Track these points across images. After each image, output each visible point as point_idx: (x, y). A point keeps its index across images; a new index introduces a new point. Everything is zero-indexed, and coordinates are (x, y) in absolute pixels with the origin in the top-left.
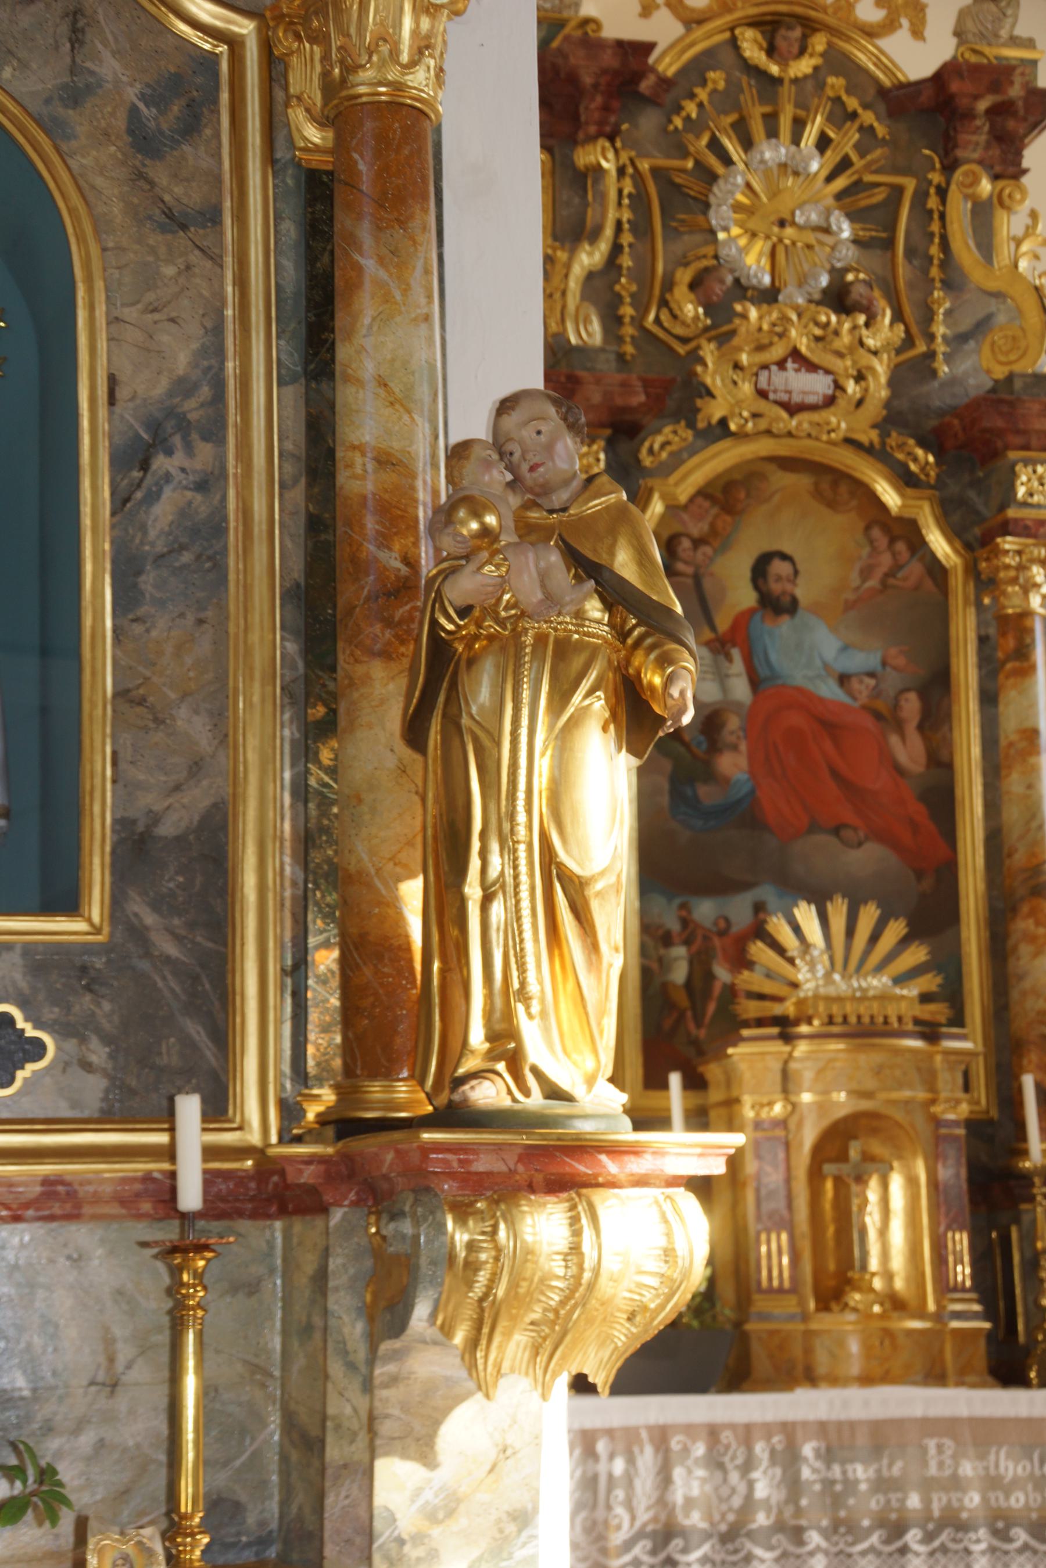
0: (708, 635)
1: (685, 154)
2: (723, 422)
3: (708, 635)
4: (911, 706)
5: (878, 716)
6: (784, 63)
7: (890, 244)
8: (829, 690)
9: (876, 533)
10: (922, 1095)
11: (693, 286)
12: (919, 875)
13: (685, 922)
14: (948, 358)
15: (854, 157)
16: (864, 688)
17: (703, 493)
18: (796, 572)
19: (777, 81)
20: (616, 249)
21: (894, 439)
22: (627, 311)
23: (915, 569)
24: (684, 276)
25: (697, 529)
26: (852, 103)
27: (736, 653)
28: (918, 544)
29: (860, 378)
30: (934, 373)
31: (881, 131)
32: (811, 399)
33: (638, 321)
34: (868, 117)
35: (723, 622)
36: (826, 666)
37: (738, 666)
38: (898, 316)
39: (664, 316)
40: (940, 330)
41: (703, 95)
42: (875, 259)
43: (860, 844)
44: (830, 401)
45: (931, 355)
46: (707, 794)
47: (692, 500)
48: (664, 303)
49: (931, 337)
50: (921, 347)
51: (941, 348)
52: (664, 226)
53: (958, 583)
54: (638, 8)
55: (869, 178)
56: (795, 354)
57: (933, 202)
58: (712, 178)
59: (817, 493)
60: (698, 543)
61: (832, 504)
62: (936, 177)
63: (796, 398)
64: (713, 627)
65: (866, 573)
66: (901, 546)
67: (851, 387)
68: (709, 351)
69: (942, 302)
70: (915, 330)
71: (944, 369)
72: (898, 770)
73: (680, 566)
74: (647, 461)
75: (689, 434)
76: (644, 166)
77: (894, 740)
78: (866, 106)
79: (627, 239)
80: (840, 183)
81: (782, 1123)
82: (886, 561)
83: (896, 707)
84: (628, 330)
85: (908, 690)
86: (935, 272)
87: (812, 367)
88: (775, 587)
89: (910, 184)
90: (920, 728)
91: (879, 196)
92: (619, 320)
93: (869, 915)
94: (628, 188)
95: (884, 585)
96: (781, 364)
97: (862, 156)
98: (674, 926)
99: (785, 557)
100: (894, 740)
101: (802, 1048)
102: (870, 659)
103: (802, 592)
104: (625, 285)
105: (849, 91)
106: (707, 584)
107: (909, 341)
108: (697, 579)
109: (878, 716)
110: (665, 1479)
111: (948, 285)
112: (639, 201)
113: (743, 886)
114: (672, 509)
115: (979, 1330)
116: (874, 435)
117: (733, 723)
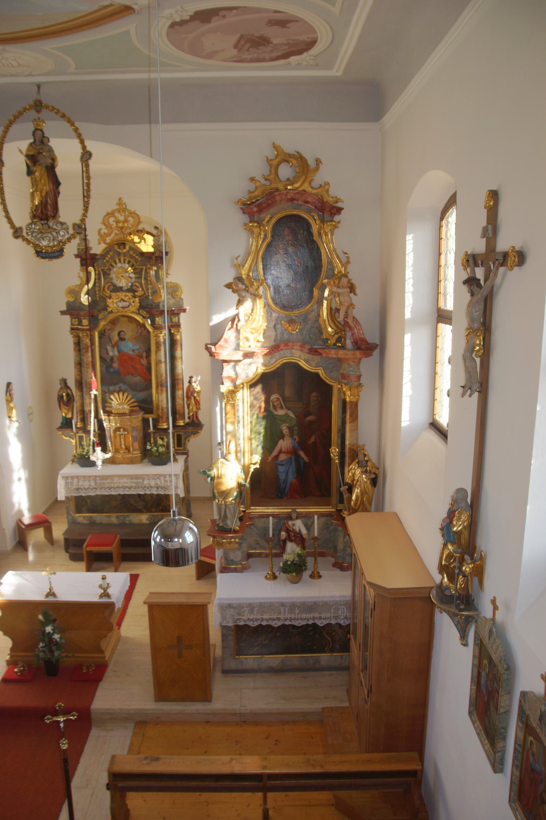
0: (111, 345)
1: (106, 267)
2: (112, 311)
3: (111, 345)
4: (144, 354)
5: (139, 356)
6: (122, 250)
7: (141, 278)
8: (131, 353)
9: (139, 326)
10: (130, 424)
11: (108, 288)
12: (146, 381)
13: (108, 390)
14: (151, 296)
15: (135, 264)
16: (136, 352)
17: (110, 322)
18: (125, 334)
19: (120, 253)
20: (95, 283)
21: (141, 311)
22: (97, 292)
23: (145, 332)
24: (107, 286)
25: (109, 328)
26: (134, 255)
27: (116, 347)
28: (145, 328)
29: (134, 302)
30: (149, 299)
31: (139, 259)
32: (126, 306)
33: (99, 294)
34: (137, 257)
35: (113, 342)
36: (130, 349)
37: (116, 350)
38: (143, 290)
39: (104, 293)
40: (150, 291)
41: (109, 256)
42: (138, 280)
43: (136, 377)
44: (129, 306)
45: (148, 296)
46: (111, 370)
47: (108, 323)
48: (104, 290)
49: (148, 293)
50: (147, 294)
51: (150, 294)
52: (104, 278)
53: (152, 335)
54: (98, 243)
55: (137, 267)
56: (122, 300)
57: (148, 271)
58: (110, 270)
59: (128, 321)
60: (109, 330)
61: (131, 322)
62: (149, 266)
63: (123, 306)
64: (111, 343)
65: (137, 333)
66: (143, 329)
67: (132, 303)
68: (108, 300)
69: (149, 286)
70: (146, 292)
71: (150, 298)
72: (142, 365)
73: (106, 334)
74: (100, 318)
75: (106, 313)
76: (100, 269)
77: (142, 360)
78: (137, 255)
79: (97, 281)
80: (133, 268)
81: (110, 428)
82: (140, 331)
83: (142, 355)
84: (98, 296)
85: (144, 352)
86: (149, 282)
87: (125, 301)
88: (122, 336)
89: (144, 268)
90: (146, 358)
91: (138, 270)
92: (96, 294)
93: (126, 395)
94: (97, 272)
95: (140, 335)
96: (120, 301)
97: (136, 263)
98: (107, 390)
99: (123, 331)
100: (142, 360)
101: (111, 418)
102: (136, 347)
103: (126, 337)
104: (97, 289)
105: (134, 253)
106: (111, 337)
107: (145, 293)
108: (109, 336)
109: (139, 356)
110: (78, 482)
111: (151, 284)
112: (99, 275)
113: (117, 384)
114: (104, 325)
115: (138, 456)
116: (138, 312)
117: (115, 359)
